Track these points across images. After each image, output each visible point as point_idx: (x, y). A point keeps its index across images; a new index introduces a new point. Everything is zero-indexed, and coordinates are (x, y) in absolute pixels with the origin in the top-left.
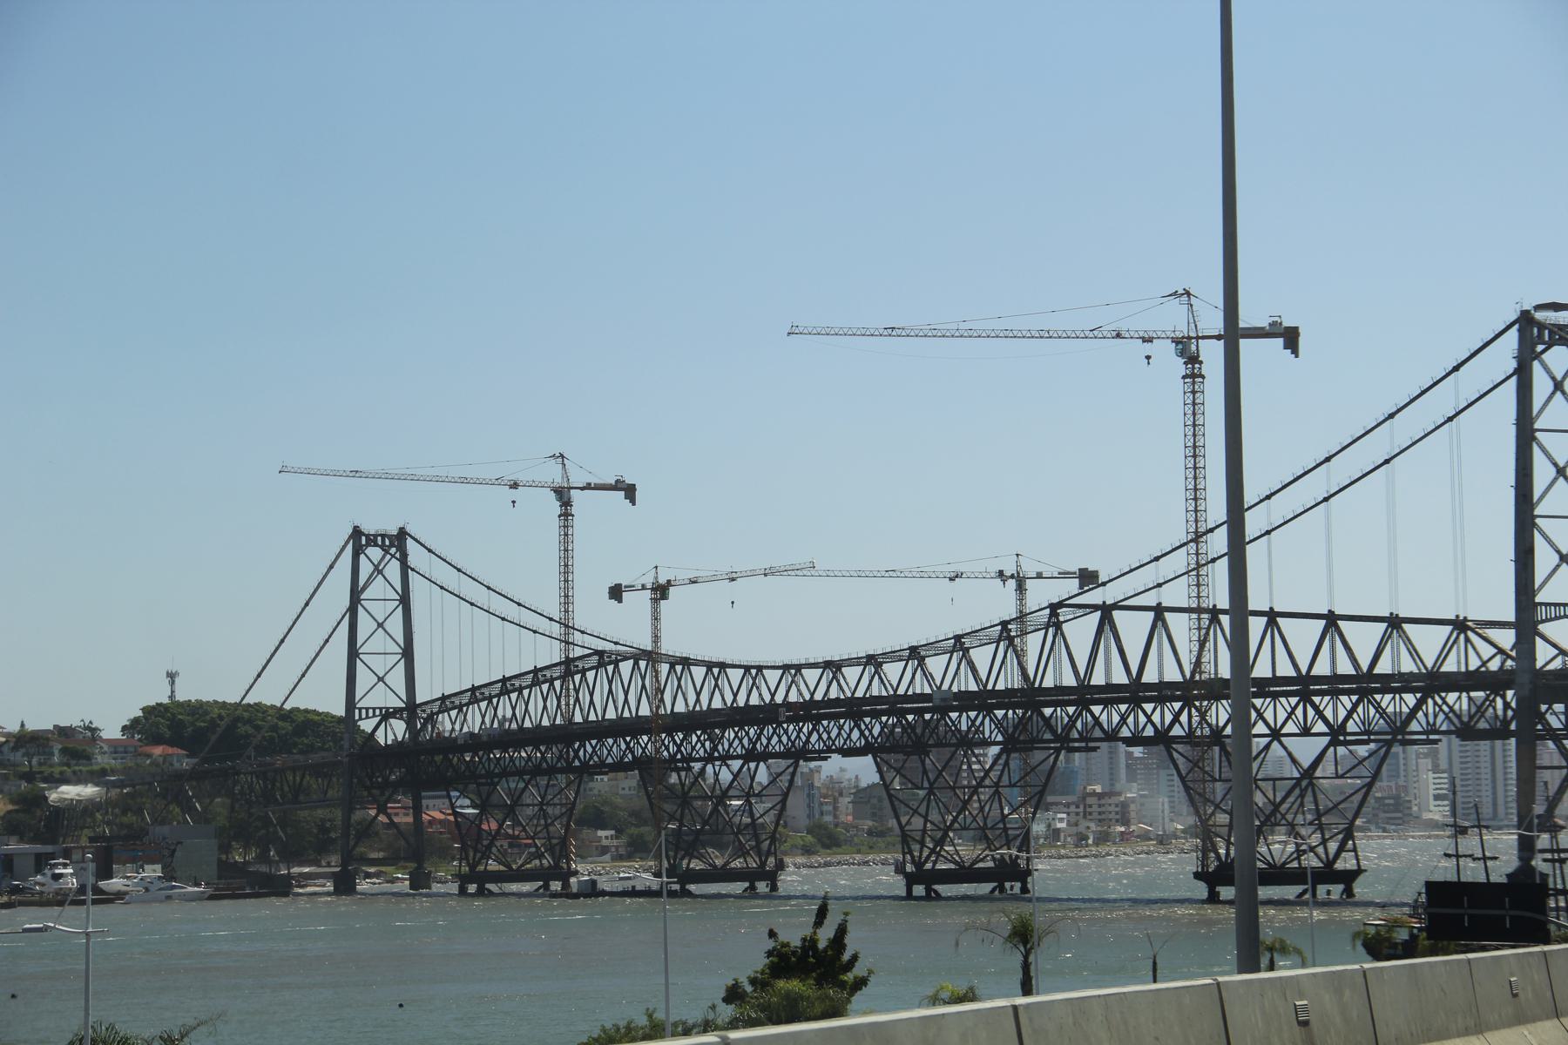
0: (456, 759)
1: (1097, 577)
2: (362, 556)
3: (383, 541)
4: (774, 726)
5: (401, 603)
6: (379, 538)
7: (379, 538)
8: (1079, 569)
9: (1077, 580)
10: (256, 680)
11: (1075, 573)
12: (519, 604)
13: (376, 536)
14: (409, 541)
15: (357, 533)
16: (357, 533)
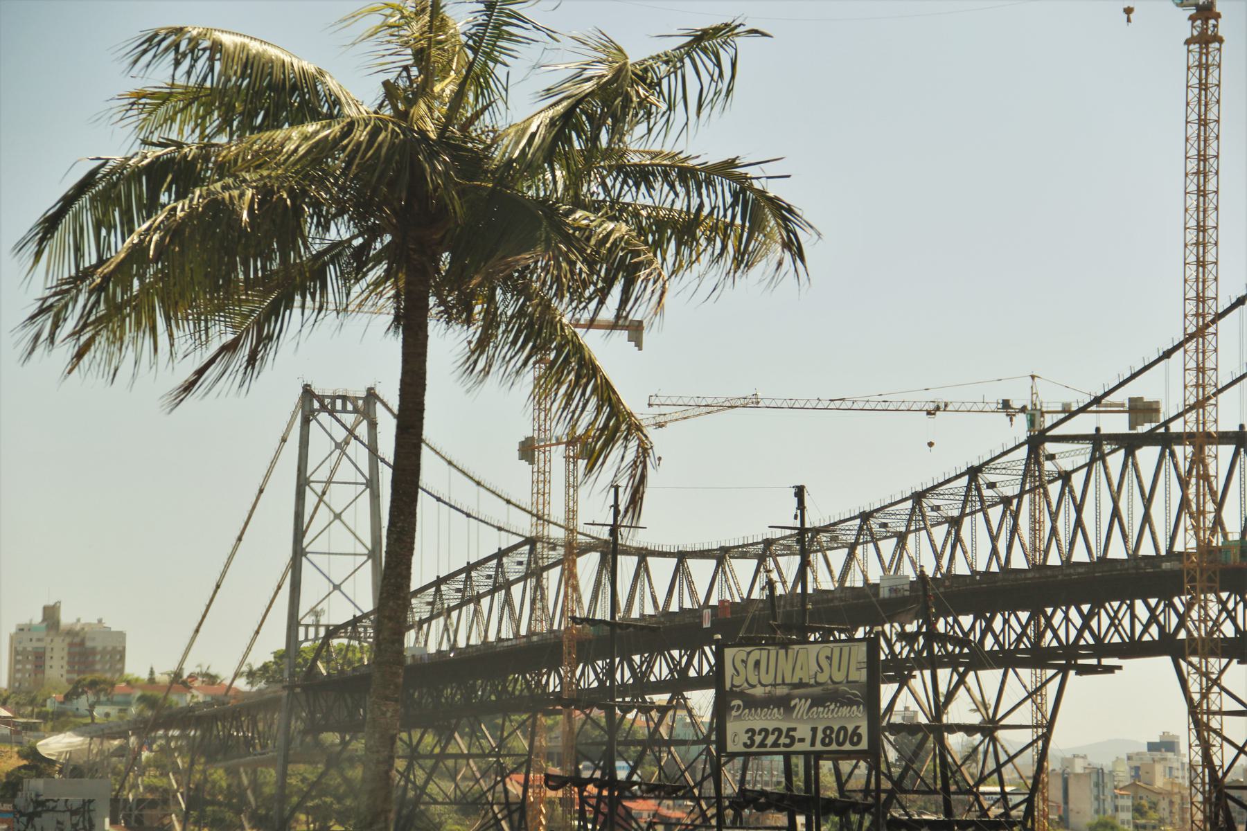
0: (416, 694)
1: (1157, 411)
2: (313, 424)
3: (344, 405)
4: (1086, 608)
5: (367, 487)
6: (339, 403)
7: (339, 403)
8: (1131, 400)
9: (1127, 415)
10: (215, 592)
11: (1123, 405)
12: (478, 483)
13: (334, 398)
14: (379, 405)
15: (308, 393)
16: (308, 393)
